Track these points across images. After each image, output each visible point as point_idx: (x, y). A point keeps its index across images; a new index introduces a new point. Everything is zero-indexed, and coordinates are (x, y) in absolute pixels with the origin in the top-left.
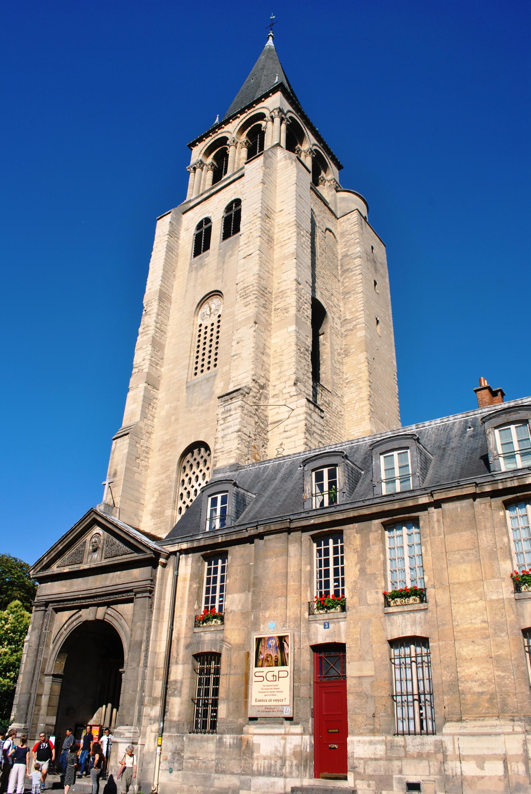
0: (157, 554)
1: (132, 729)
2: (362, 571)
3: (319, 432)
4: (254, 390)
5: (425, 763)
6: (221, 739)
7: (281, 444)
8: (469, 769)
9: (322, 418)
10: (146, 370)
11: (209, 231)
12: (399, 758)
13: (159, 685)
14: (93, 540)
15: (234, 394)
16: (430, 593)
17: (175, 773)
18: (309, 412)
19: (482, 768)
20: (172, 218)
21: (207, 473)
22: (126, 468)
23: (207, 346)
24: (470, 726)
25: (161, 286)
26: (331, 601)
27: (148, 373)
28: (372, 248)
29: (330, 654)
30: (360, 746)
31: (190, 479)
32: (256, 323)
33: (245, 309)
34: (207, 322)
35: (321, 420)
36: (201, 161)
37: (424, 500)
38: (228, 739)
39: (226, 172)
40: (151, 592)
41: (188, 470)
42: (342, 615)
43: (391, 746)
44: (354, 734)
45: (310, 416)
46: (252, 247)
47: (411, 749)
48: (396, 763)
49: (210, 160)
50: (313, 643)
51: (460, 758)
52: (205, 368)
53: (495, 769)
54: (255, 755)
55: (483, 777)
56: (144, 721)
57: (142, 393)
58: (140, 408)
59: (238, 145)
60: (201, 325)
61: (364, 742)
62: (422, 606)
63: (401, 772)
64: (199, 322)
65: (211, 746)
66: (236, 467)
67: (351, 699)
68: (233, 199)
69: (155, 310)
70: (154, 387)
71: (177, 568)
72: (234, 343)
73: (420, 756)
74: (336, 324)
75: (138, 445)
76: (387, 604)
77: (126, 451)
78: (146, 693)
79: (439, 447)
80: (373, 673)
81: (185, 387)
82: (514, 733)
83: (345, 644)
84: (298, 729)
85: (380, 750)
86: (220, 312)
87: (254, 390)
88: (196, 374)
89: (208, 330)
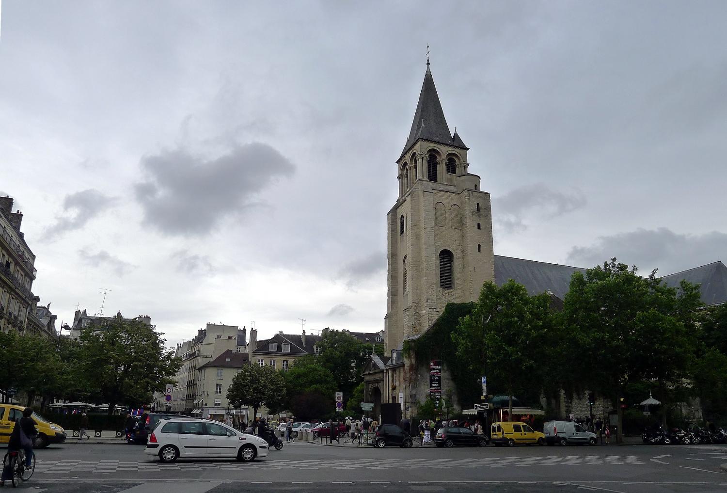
28: (478, 204)
74: (459, 254)
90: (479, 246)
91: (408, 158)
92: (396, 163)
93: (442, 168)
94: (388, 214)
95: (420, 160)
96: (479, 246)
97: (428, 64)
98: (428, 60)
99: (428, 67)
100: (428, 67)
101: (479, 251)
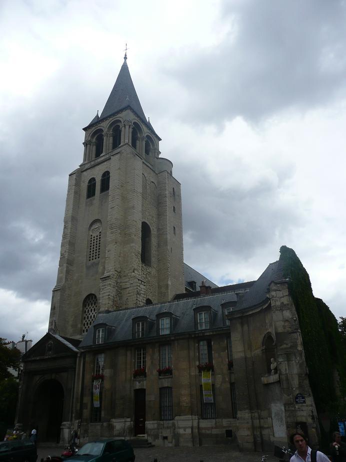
0: (77, 353)
1: (69, 423)
2: (152, 362)
3: (143, 293)
4: (115, 275)
5: (169, 430)
6: (102, 425)
7: (127, 299)
8: (181, 431)
9: (145, 285)
10: (66, 257)
11: (95, 185)
12: (161, 429)
13: (79, 405)
14: (49, 346)
15: (108, 278)
16: (173, 371)
17: (86, 438)
18: (139, 285)
19: (185, 431)
20: (77, 176)
21: (96, 308)
22: (60, 306)
23: (95, 247)
24: (182, 417)
25: (72, 213)
26: (140, 373)
27: (68, 259)
29: (140, 393)
30: (150, 424)
31: (88, 310)
32: (116, 243)
33: (111, 235)
34: (94, 235)
35: (144, 287)
36: (90, 141)
37: (173, 338)
38: (105, 424)
39: (102, 152)
40: (75, 368)
41: (87, 307)
42: (144, 379)
43: (159, 425)
44: (147, 421)
45: (139, 286)
46: (114, 203)
47: (165, 426)
48: (160, 430)
49: (94, 140)
50: (135, 389)
51: (179, 428)
52: (94, 258)
53: (189, 431)
54: (115, 430)
55: (185, 434)
56: (73, 419)
57: (65, 269)
58: (64, 276)
59: (109, 135)
60: (92, 236)
61: (151, 424)
62: (171, 376)
63: (162, 433)
64: (91, 234)
65: (99, 427)
66: (108, 312)
67: (147, 407)
68: (106, 170)
69: (70, 227)
70: (70, 265)
71: (84, 358)
72: (107, 251)
73: (168, 428)
75: (65, 295)
76: (160, 375)
77: (59, 298)
78: (74, 409)
79: (183, 313)
80: (153, 399)
81: (85, 266)
82: (195, 419)
83: (145, 390)
84: (129, 420)
85: (156, 426)
86: (100, 231)
87: (115, 275)
88: (90, 260)
89: (95, 238)
90: (174, 228)
91: (105, 126)
92: (84, 129)
93: (141, 144)
94: (70, 175)
95: (123, 129)
96: (174, 228)
97: (125, 58)
98: (126, 55)
99: (125, 60)
100: (125, 60)
101: (175, 233)
